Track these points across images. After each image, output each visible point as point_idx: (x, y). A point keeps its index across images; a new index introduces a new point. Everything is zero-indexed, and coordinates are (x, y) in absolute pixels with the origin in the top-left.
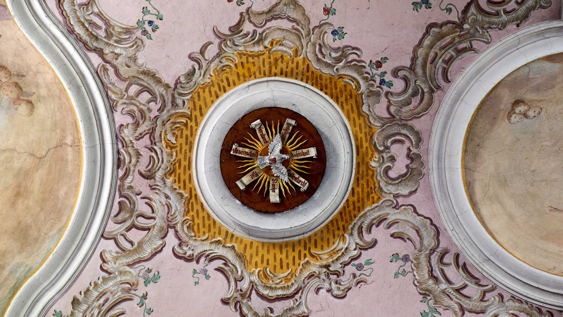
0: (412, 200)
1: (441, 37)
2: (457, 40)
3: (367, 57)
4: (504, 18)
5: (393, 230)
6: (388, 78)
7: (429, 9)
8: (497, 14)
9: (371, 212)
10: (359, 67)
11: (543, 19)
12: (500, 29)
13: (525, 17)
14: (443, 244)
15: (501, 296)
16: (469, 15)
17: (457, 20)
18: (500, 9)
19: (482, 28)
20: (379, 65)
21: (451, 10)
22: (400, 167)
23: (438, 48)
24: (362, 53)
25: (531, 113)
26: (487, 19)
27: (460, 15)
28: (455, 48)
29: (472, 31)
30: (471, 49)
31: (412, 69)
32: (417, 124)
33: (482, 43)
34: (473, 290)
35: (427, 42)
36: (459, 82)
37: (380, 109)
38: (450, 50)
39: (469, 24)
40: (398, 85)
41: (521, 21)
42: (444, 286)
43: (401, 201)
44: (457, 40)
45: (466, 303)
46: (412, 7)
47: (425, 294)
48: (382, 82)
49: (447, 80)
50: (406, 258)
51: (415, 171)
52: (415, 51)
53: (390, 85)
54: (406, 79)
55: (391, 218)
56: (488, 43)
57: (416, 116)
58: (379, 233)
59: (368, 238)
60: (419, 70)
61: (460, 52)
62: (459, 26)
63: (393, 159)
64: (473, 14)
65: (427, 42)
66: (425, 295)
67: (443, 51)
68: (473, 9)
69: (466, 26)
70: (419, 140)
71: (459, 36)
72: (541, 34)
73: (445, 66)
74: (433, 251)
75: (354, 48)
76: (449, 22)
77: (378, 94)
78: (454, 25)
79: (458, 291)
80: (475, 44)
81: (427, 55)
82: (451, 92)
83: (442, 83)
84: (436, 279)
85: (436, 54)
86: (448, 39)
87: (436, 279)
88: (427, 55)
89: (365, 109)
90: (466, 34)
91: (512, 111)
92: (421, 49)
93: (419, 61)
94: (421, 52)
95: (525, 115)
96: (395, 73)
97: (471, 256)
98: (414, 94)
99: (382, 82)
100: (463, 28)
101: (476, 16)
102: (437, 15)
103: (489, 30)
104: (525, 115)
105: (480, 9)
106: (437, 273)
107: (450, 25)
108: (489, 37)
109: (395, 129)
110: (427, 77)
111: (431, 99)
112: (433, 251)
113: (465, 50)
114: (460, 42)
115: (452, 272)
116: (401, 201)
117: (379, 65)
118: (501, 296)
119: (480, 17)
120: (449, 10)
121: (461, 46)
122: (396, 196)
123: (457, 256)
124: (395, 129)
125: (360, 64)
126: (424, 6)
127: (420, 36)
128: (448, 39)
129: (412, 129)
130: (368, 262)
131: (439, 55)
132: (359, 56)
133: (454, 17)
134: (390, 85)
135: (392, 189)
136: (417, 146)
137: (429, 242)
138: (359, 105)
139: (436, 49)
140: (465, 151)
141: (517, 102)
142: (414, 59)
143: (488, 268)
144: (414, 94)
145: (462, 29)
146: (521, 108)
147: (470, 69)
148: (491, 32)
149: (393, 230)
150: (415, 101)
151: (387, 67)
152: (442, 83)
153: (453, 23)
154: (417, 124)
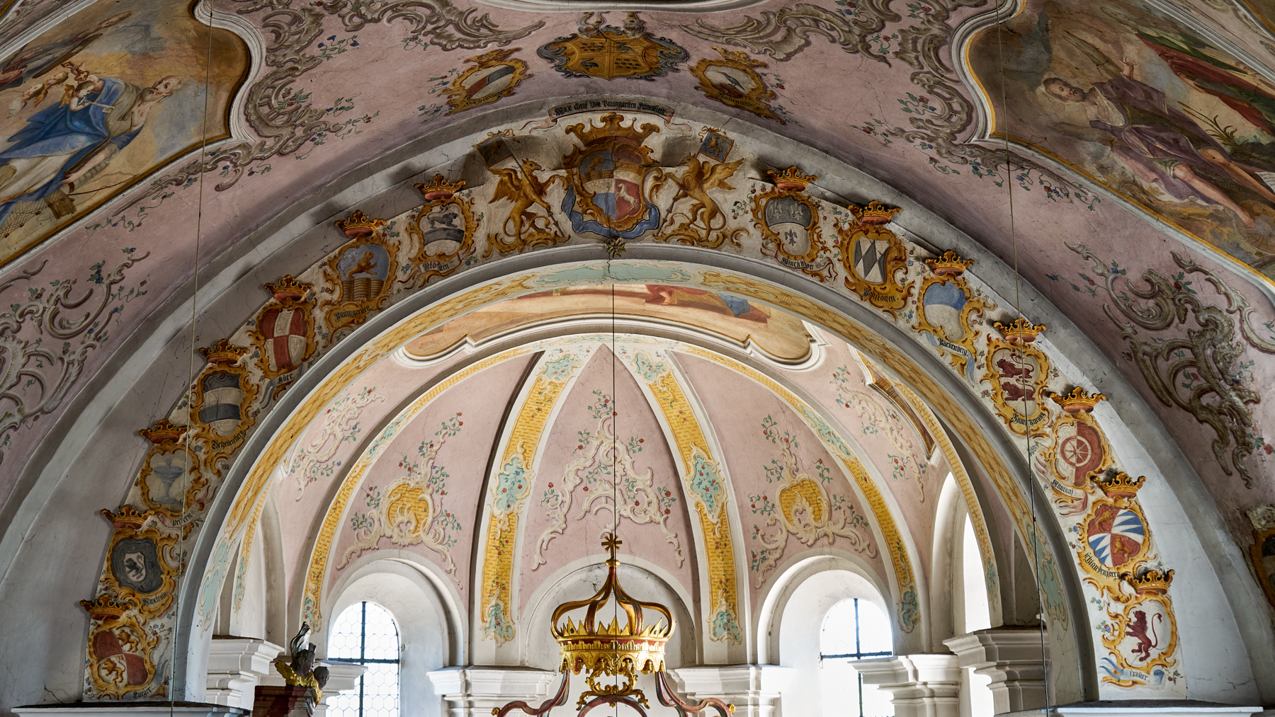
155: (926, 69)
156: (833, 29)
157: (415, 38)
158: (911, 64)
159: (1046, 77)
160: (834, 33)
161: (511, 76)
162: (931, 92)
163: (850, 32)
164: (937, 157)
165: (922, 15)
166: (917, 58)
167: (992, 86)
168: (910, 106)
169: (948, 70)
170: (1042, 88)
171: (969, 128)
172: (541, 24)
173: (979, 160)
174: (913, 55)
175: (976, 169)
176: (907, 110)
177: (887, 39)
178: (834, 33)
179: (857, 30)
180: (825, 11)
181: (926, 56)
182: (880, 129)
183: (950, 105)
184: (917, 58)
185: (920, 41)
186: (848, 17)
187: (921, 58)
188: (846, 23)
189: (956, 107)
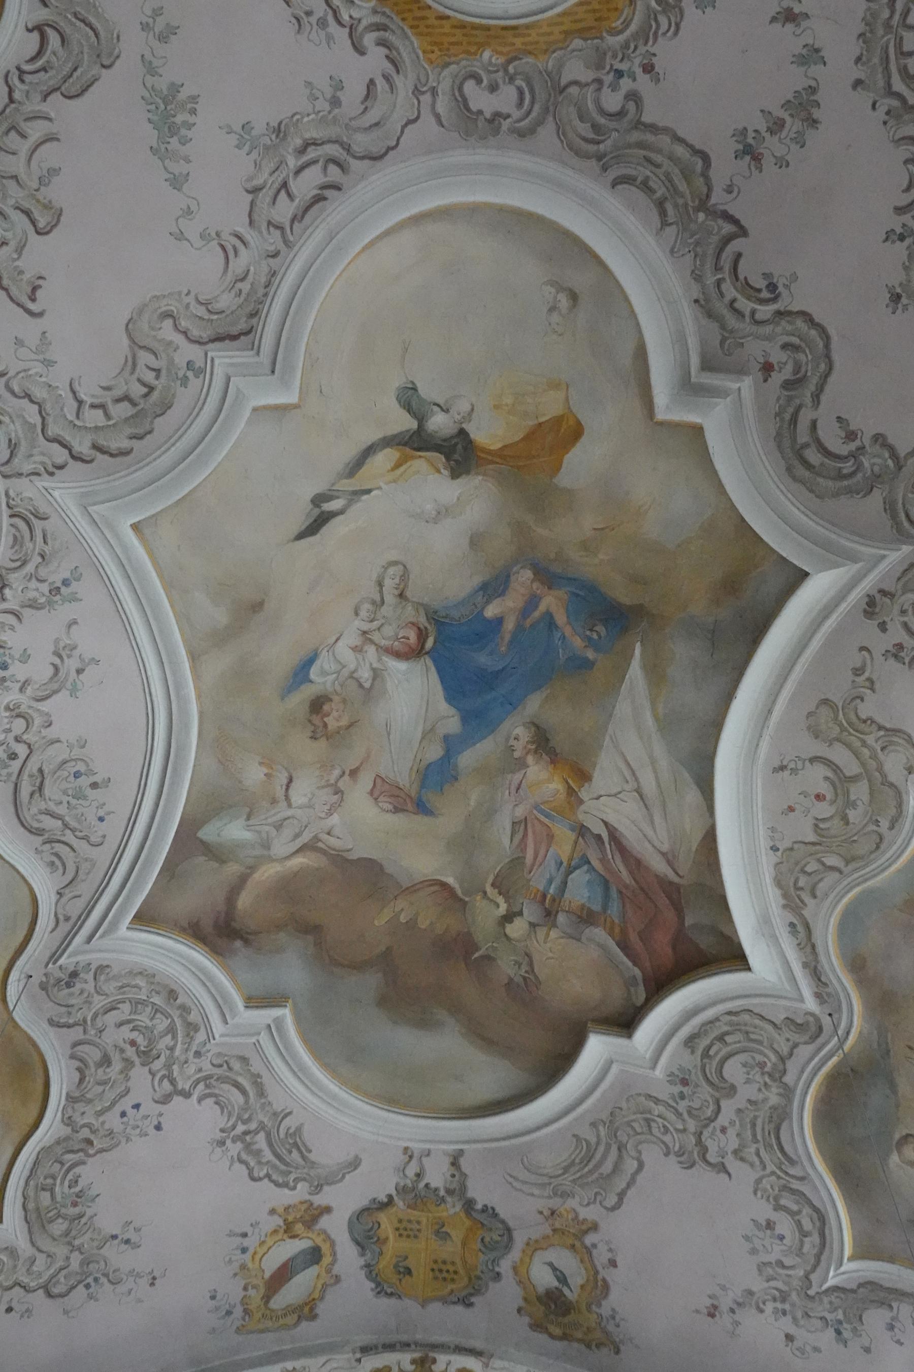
0: (427, 118)
1: (687, 175)
2: (681, 201)
3: (663, 51)
4: (710, 280)
5: (380, 83)
6: (626, 84)
7: (734, 155)
8: (718, 268)
9: (409, 47)
10: (646, 34)
11: (703, 343)
12: (693, 272)
13: (710, 314)
14: (354, 164)
15: (275, 255)
16: (720, 221)
17: (713, 200)
18: (726, 274)
19: (697, 244)
20: (648, 69)
21: (730, 192)
22: (480, 100)
23: (670, 170)
24: (671, 39)
25: (555, 318)
26: (711, 251)
27: (722, 207)
28: (666, 198)
29: (693, 226)
30: (665, 224)
31: (638, 125)
32: (547, 132)
33: (672, 243)
34: (284, 210)
35: (680, 151)
36: (613, 202)
37: (576, 70)
38: (664, 189)
39: (703, 222)
40: (613, 101)
41: (704, 306)
42: (292, 162)
43: (426, 99)
44: (681, 201)
45: (265, 197)
46: (740, 127)
47: (279, 131)
48: (619, 74)
49: (615, 184)
50: (335, 102)
51: (475, 126)
52: (666, 130)
53: (614, 87)
54: (621, 114)
55: (398, 80)
56: (672, 251)
57: (560, 131)
58: (376, 59)
59: (369, 40)
60: (636, 136)
61: (660, 205)
62: (703, 205)
63: (493, 88)
64: (720, 228)
65: (680, 151)
66: (278, 130)
67: (663, 178)
68: (728, 228)
69: (701, 216)
70: (522, 134)
71: (686, 205)
72: (680, 339)
73: (640, 179)
74: (348, 149)
75: (678, 26)
76: (710, 189)
77: (599, 66)
78: (704, 197)
79: (285, 185)
80: (671, 231)
81: (659, 151)
82: (599, 191)
83: (613, 174)
84: (302, 151)
85: (658, 166)
86: (682, 186)
87: (302, 151)
88: (659, 151)
89: (577, 43)
90: (689, 216)
91: (560, 288)
92: (669, 140)
93: (649, 138)
94: (664, 141)
95: (552, 309)
96: (633, 96)
97: (336, 211)
98: (595, 127)
99: (619, 74)
100: (699, 211)
101: (717, 233)
102: (724, 167)
103: (692, 253)
104: (552, 309)
105: (728, 240)
106: (312, 153)
107: (705, 190)
108: (681, 253)
109: (541, 95)
110: (626, 151)
111: (587, 156)
112: (348, 149)
113: (663, 213)
114: (676, 206)
115: (313, 178)
116: (426, 99)
117: (648, 69)
118: (275, 255)
119: (715, 239)
120: (729, 190)
121: (669, 207)
122: (434, 92)
123: (338, 188)
124: (541, 95)
125: (651, 36)
126: (741, 147)
127: (690, 140)
128: (682, 186)
129: (540, 122)
130: (330, 38)
131: (658, 171)
132: (664, 34)
133: (718, 198)
134: (614, 87)
135: (445, 86)
136: (513, 131)
137: (362, 142)
138: (583, 33)
139: (667, 165)
140: (502, 210)
141: (574, 297)
142: (653, 128)
143: (319, 235)
144: (595, 127)
145: (698, 210)
146: (564, 301)
147: (631, 222)
148: (689, 258)
149: (380, 83)
150: (584, 129)
151: (643, 83)
152: (613, 174)
153: (708, 196)
154: (547, 132)
155: (771, 1167)
156: (666, 1131)
157: (222, 1143)
158: (752, 1165)
159: (897, 1136)
160: (667, 1139)
161: (313, 1271)
162: (778, 1207)
163: (684, 1130)
164: (792, 1330)
165: (758, 1077)
166: (758, 1154)
167: (845, 1174)
168: (757, 1243)
169: (792, 1162)
170: (895, 1158)
171: (827, 1249)
172: (355, 1164)
173: (840, 1316)
174: (752, 1150)
175: (838, 1332)
176: (754, 1251)
177: (723, 1130)
178: (667, 1139)
179: (692, 1125)
180: (657, 1101)
181: (768, 1146)
182: (725, 1303)
183: (799, 1224)
184: (758, 1154)
185: (759, 1122)
186: (682, 1106)
187: (762, 1152)
188: (679, 1114)
189: (807, 1225)
